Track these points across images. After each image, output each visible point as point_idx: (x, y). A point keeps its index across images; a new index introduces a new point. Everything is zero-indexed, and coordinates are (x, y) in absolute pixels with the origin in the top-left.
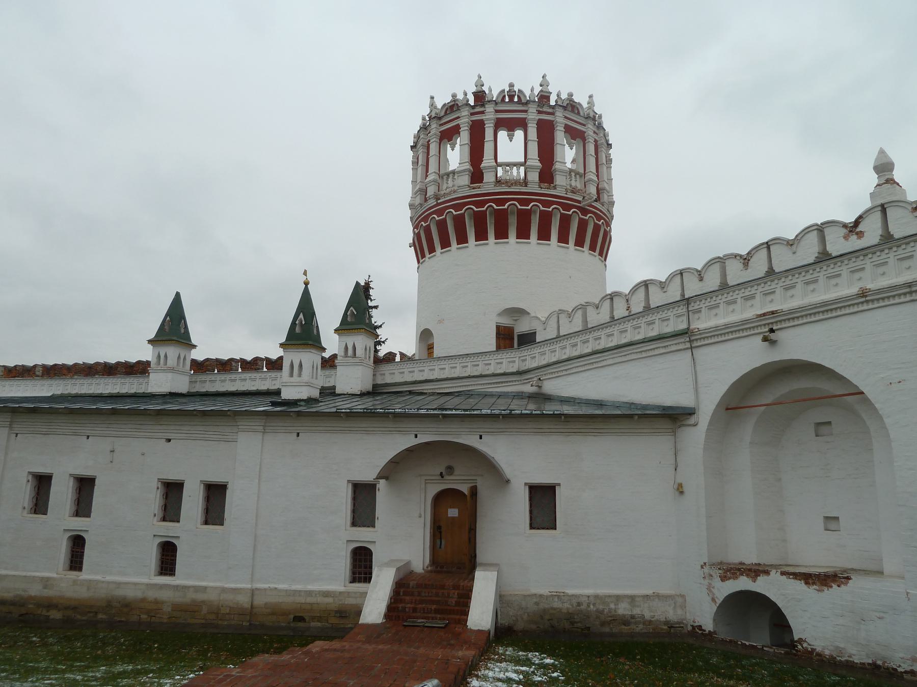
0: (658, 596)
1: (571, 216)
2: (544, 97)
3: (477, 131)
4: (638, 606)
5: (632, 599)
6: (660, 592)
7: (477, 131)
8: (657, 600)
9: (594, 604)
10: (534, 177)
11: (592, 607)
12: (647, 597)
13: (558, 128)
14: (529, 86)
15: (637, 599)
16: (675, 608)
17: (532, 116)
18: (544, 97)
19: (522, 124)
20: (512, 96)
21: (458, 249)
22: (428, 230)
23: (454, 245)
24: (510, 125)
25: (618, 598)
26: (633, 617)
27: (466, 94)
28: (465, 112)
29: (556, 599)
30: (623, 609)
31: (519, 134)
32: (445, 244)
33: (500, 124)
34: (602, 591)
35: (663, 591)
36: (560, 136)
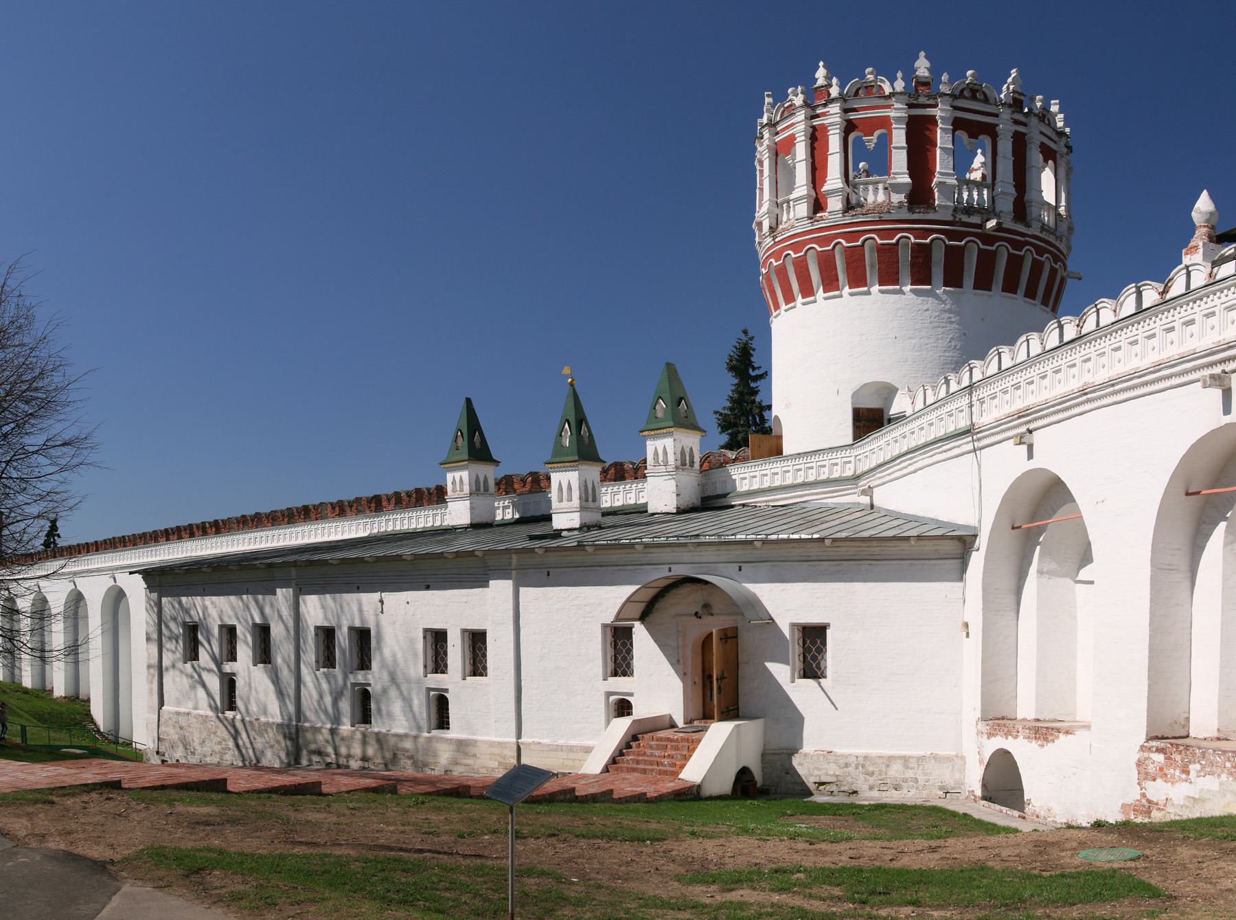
0: (936, 758)
4: (911, 768)
5: (905, 759)
6: (939, 753)
8: (933, 761)
9: (863, 766)
11: (861, 768)
12: (921, 759)
15: (911, 760)
16: (952, 770)
21: (826, 299)
23: (820, 294)
25: (891, 759)
26: (905, 780)
29: (822, 759)
30: (896, 771)
32: (807, 291)
34: (873, 751)
35: (941, 752)
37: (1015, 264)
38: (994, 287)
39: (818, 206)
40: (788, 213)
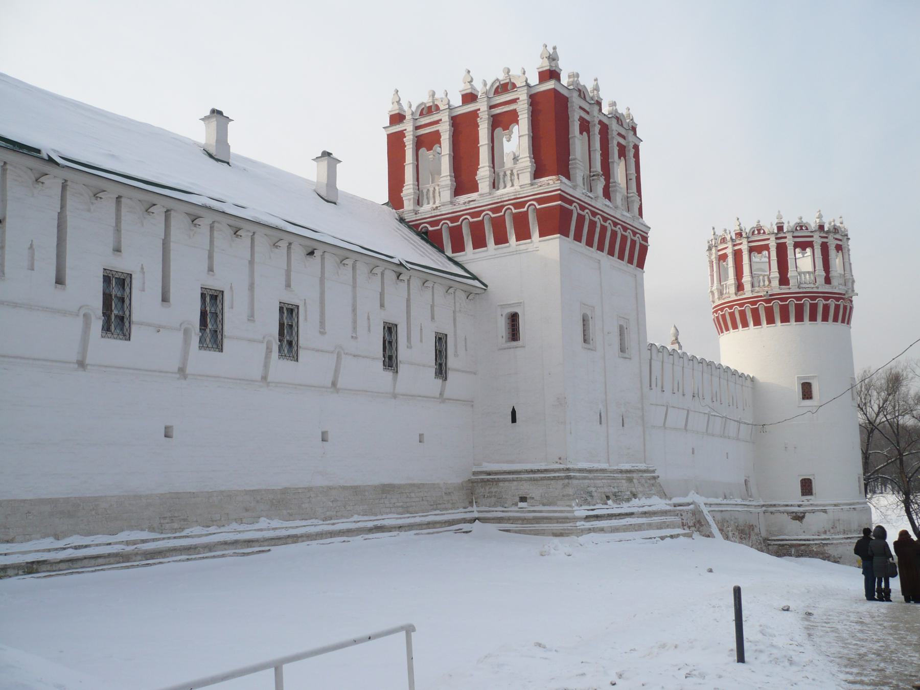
1: (817, 303)
2: (821, 227)
3: (782, 250)
7: (782, 250)
10: (821, 280)
13: (831, 248)
14: (812, 222)
17: (817, 240)
18: (821, 227)
19: (810, 245)
20: (801, 226)
22: (724, 316)
24: (802, 245)
27: (772, 225)
28: (773, 238)
31: (809, 251)
33: (796, 245)
36: (832, 252)
37: (826, 308)
38: (829, 320)
39: (740, 287)
40: (726, 289)
